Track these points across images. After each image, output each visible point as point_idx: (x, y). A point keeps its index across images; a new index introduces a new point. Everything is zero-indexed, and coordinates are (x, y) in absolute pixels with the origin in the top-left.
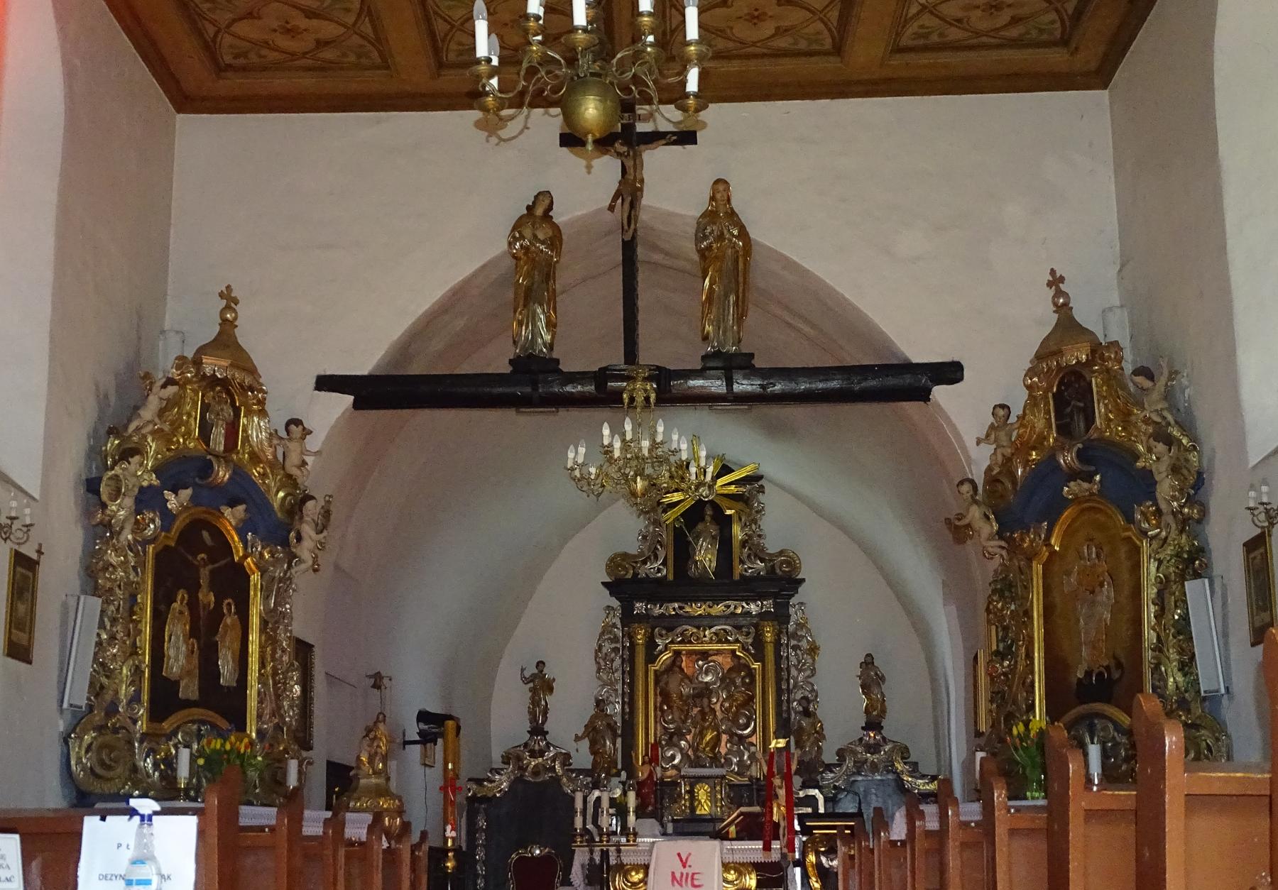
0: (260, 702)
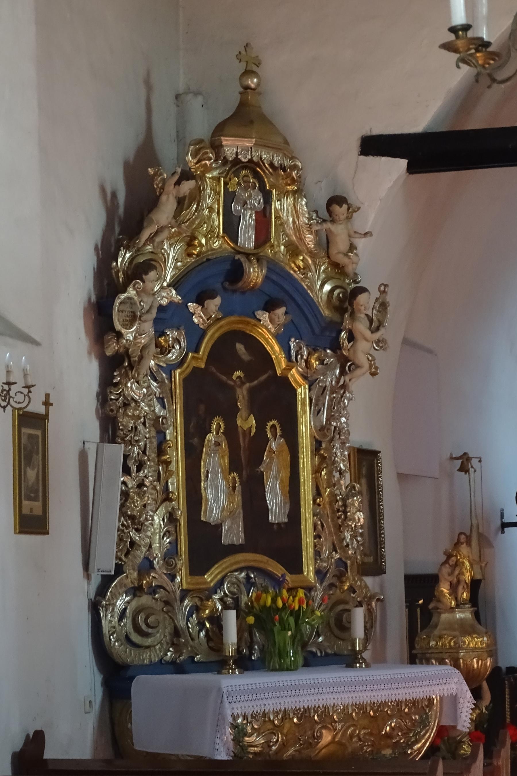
0: (318, 536)
